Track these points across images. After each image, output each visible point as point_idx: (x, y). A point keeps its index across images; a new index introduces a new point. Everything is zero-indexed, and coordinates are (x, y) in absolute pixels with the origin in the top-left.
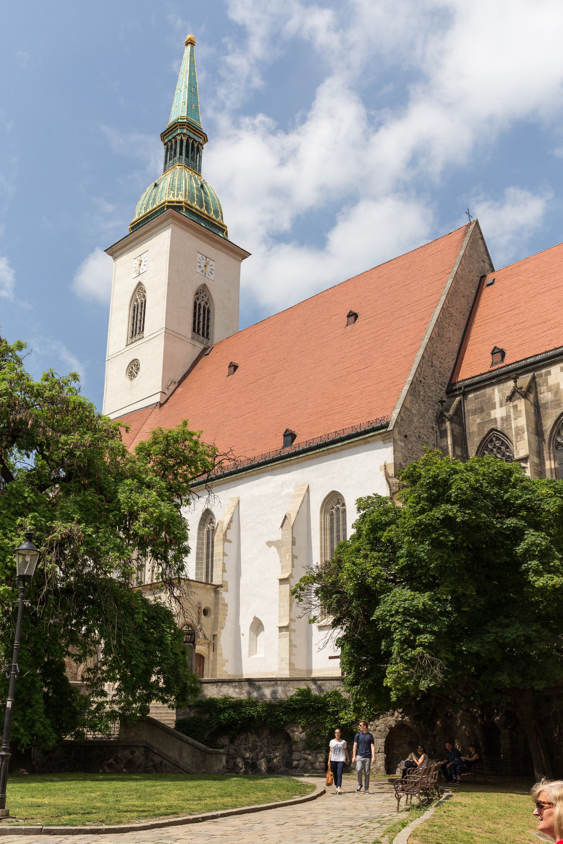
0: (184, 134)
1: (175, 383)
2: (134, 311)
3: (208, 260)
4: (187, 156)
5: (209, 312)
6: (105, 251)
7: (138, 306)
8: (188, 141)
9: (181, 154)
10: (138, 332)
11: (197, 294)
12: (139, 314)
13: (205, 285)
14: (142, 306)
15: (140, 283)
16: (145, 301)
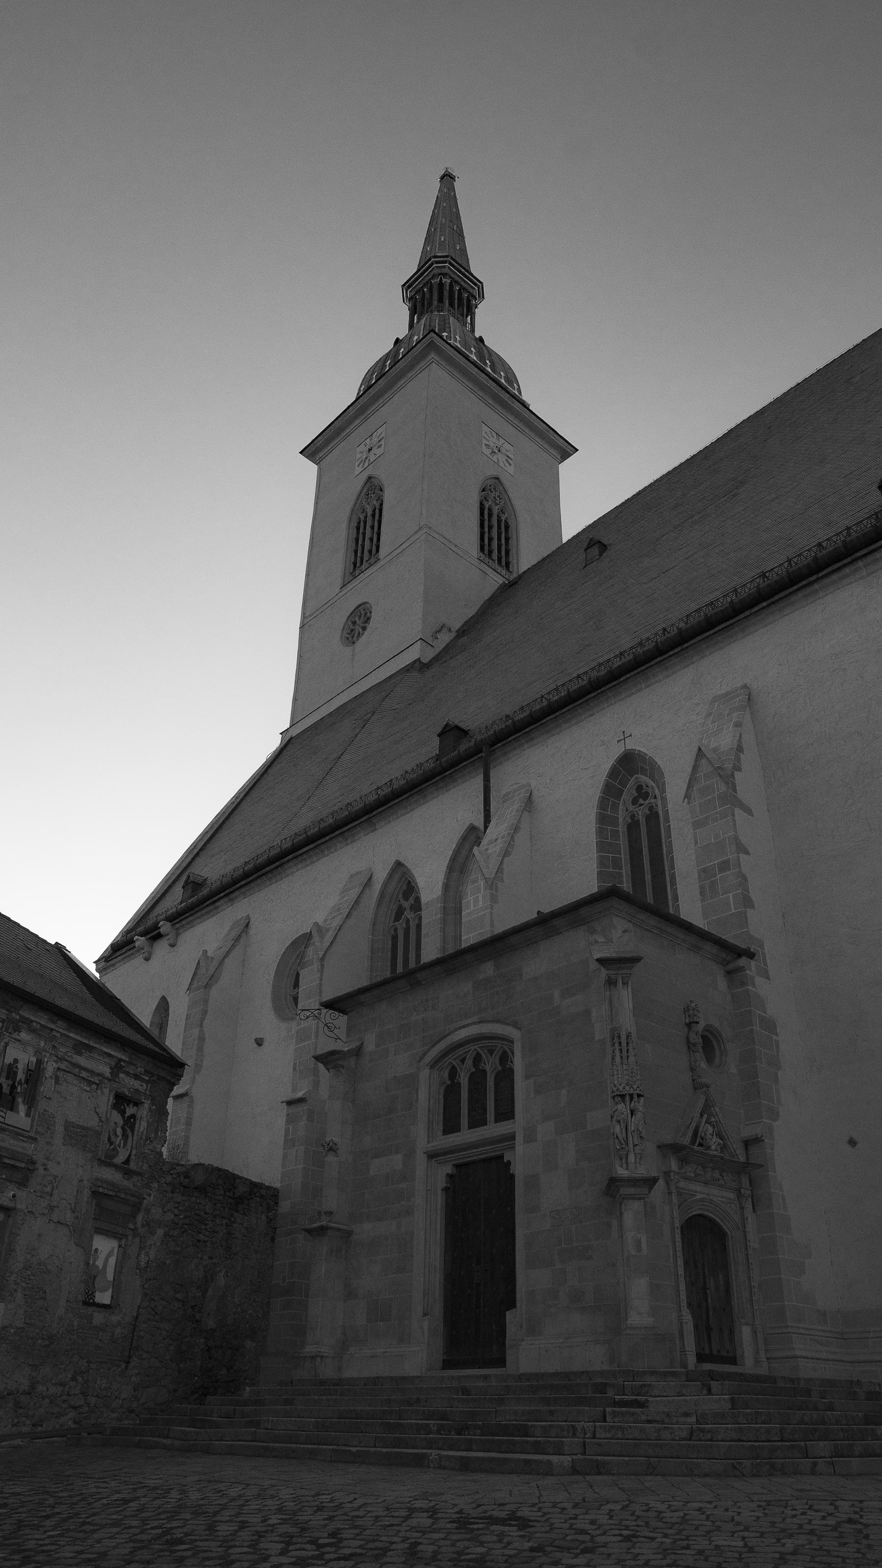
0: (445, 275)
1: (450, 630)
2: (358, 528)
3: (502, 441)
4: (451, 304)
5: (507, 527)
6: (301, 453)
7: (366, 517)
8: (451, 285)
9: (441, 300)
10: (365, 558)
11: (483, 490)
12: (367, 542)
13: (497, 478)
14: (373, 516)
15: (370, 478)
16: (381, 505)
